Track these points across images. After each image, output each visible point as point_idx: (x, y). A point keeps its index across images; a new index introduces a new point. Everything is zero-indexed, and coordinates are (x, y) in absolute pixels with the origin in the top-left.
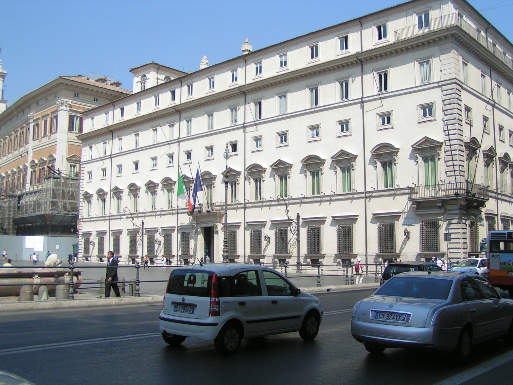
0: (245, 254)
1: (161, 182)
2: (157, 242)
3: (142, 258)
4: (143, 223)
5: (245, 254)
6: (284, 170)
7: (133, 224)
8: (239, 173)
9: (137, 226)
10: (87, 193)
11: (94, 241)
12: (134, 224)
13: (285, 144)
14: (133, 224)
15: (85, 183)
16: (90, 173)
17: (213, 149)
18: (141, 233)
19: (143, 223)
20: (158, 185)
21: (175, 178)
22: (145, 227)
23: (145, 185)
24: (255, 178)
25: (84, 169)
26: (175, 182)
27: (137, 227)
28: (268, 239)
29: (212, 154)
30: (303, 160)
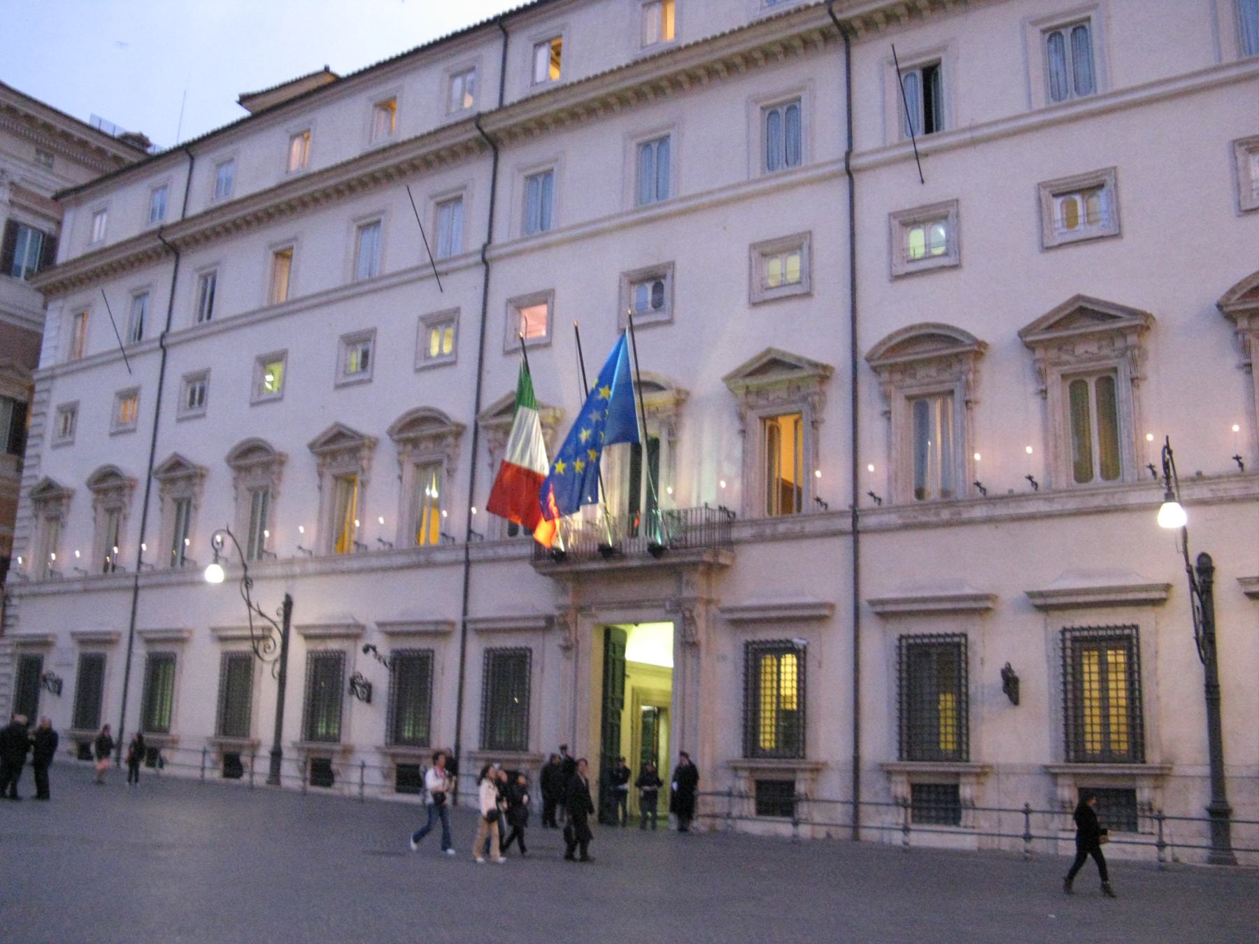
0: (856, 759)
1: (391, 433)
2: (358, 688)
3: (277, 755)
4: (288, 605)
5: (856, 759)
6: (1099, 348)
7: (249, 605)
8: (823, 374)
9: (262, 614)
10: (49, 486)
11: (60, 673)
12: (254, 604)
13: (1095, 231)
14: (249, 605)
15: (46, 449)
16: (70, 412)
17: (666, 283)
18: (278, 651)
19: (288, 605)
20: (373, 444)
21: (460, 411)
22: (297, 618)
23: (312, 446)
24: (915, 391)
25: (44, 396)
26: (459, 431)
27: (267, 623)
28: (1011, 683)
29: (658, 304)
30: (1233, 291)
